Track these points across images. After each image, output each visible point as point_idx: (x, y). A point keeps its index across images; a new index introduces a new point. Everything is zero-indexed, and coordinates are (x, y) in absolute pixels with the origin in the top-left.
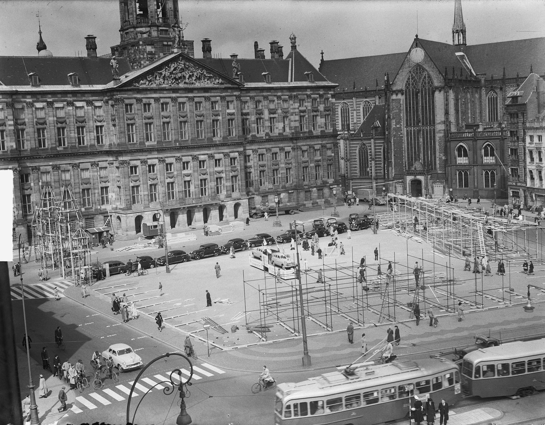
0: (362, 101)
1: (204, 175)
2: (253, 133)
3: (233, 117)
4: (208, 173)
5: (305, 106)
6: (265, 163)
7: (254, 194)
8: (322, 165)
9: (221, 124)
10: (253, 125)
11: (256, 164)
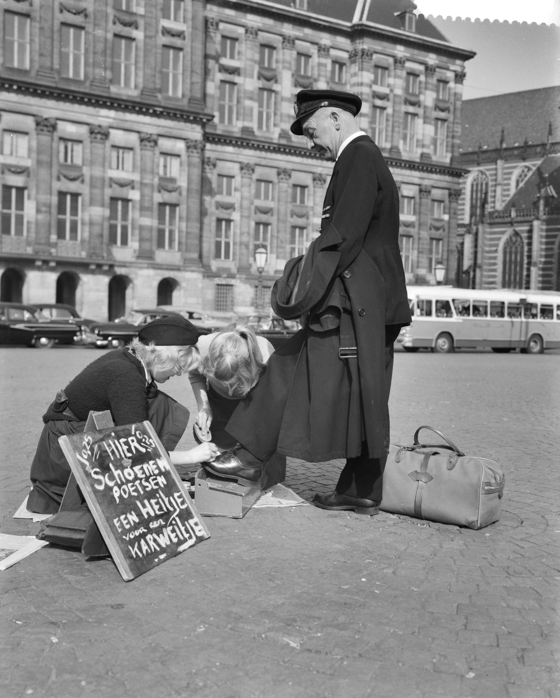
0: (515, 167)
1: (73, 180)
2: (247, 124)
3: (178, 42)
4: (87, 179)
5: (389, 86)
6: (270, 204)
7: (232, 276)
8: (416, 237)
9: (141, 54)
10: (248, 103)
11: (246, 203)
